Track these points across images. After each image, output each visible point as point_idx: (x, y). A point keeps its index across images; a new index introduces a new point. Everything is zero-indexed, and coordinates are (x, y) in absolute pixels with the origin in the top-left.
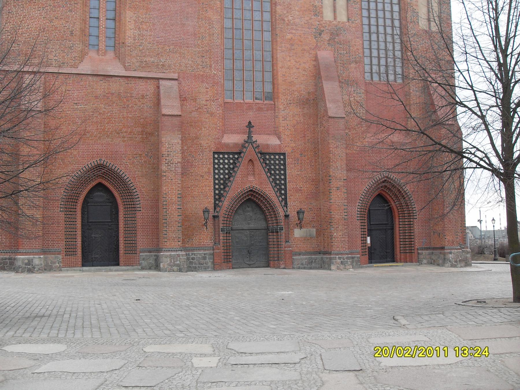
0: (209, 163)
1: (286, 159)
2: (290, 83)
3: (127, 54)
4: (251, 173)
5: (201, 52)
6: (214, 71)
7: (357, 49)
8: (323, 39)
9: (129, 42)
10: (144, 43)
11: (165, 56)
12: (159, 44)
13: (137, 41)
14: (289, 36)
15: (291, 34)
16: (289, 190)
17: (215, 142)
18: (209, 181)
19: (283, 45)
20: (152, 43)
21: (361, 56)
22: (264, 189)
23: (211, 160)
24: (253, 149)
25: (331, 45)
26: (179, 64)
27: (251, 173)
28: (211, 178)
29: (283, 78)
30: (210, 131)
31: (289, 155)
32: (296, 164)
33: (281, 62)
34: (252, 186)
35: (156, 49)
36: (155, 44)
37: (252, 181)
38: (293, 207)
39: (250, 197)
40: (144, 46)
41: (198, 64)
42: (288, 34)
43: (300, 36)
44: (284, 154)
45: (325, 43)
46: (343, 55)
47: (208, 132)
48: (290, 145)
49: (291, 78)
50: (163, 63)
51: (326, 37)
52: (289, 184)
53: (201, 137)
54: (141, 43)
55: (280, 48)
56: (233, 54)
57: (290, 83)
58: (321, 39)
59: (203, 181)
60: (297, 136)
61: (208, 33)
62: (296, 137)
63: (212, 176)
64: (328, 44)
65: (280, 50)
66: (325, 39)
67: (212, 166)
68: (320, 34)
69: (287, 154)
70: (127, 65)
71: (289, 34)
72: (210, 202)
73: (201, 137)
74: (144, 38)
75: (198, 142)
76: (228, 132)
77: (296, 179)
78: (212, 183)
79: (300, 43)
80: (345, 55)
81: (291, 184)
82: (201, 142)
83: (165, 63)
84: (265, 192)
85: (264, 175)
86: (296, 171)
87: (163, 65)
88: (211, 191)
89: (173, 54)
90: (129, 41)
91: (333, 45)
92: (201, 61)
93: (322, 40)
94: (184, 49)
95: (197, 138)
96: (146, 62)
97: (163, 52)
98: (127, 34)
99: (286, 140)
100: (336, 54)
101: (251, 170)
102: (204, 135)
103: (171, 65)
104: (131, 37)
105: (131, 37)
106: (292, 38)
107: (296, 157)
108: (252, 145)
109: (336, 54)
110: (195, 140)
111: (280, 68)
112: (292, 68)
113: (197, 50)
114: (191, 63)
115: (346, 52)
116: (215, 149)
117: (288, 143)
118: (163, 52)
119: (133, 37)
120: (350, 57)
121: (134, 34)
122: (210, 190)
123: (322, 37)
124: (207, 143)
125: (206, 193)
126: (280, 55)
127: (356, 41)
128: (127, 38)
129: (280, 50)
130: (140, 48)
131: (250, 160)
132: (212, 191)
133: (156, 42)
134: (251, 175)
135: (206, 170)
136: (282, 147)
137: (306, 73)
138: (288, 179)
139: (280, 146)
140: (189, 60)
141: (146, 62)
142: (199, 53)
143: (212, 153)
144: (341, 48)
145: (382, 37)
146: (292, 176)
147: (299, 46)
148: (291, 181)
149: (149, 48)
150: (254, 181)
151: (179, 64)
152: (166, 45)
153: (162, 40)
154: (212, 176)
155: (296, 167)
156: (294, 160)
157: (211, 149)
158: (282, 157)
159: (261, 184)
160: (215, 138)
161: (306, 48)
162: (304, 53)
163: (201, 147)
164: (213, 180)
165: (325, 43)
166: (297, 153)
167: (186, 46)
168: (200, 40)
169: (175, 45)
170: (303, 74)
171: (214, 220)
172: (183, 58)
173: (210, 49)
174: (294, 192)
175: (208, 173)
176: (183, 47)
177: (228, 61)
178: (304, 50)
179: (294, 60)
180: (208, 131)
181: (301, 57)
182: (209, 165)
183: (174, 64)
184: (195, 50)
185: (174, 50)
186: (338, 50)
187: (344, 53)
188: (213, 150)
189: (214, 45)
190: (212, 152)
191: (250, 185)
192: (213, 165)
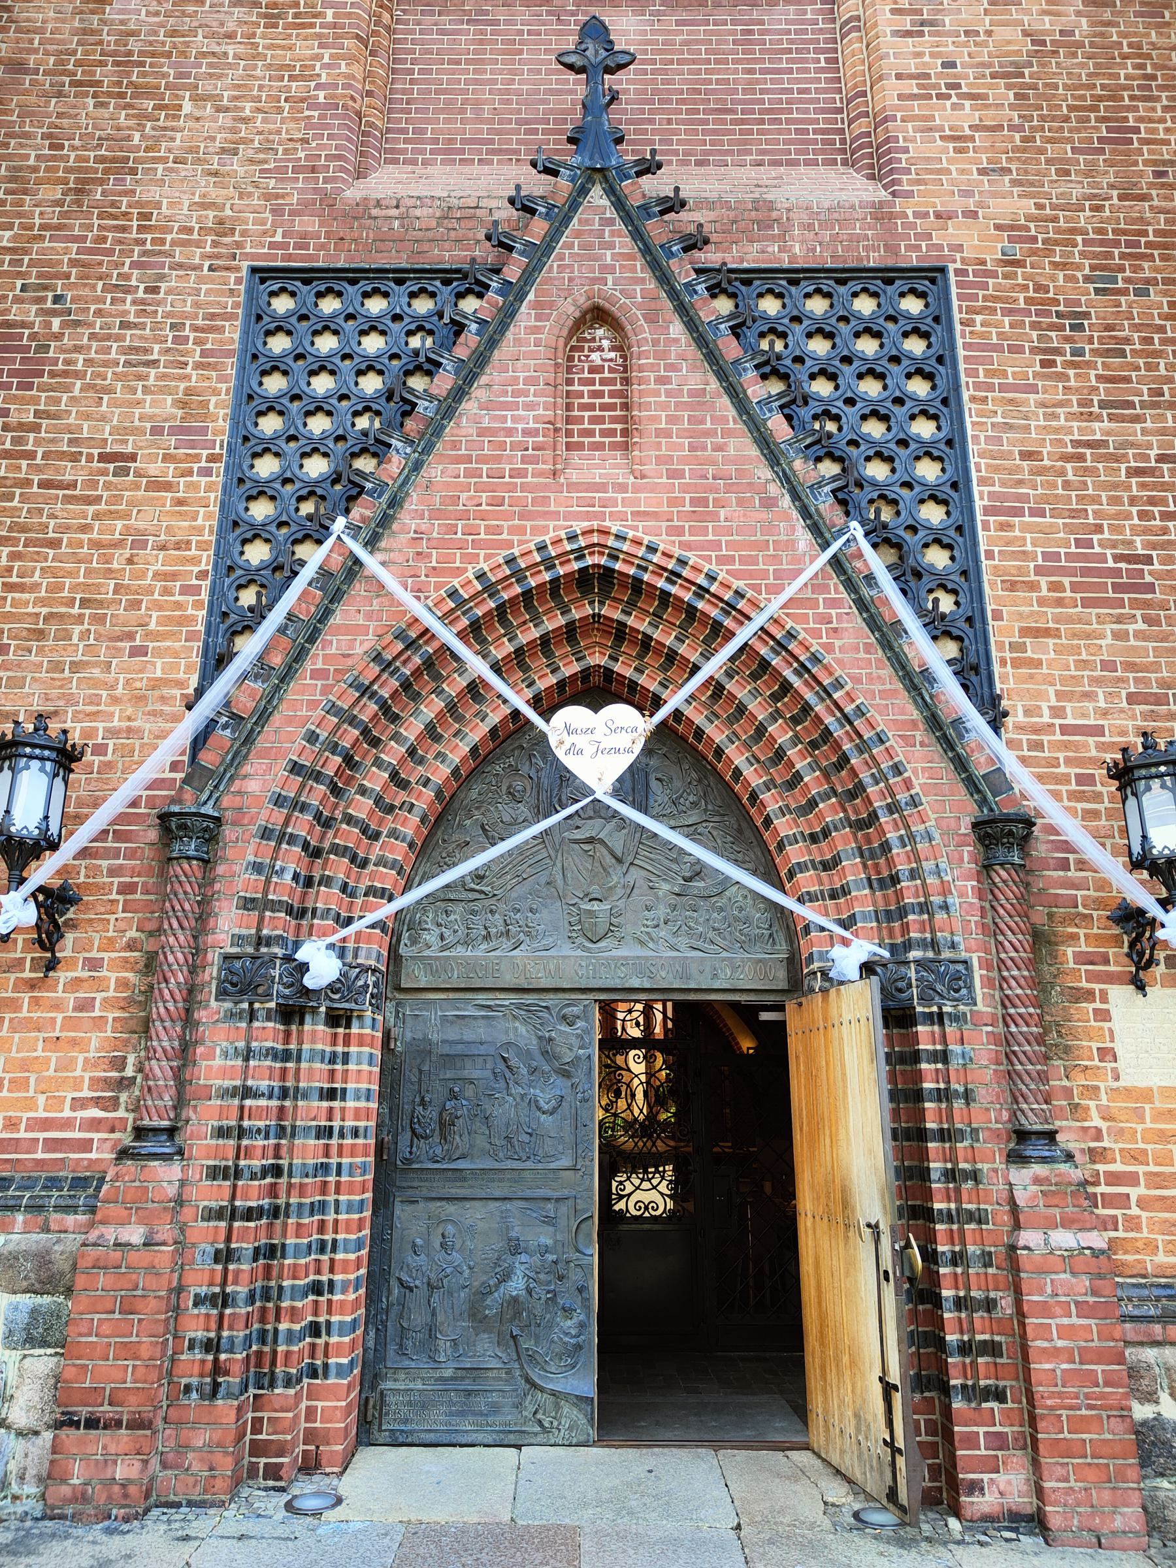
0: (203, 354)
1: (957, 316)
4: (604, 433)
16: (1012, 586)
17: (277, 196)
18: (180, 502)
22: (729, 560)
23: (220, 330)
24: (619, 225)
27: (604, 433)
28: (207, 472)
30: (245, 120)
31: (985, 286)
32: (1058, 351)
34: (604, 532)
37: (602, 488)
38: (1066, 746)
39: (597, 659)
44: (935, 274)
47: (222, 129)
48: (981, 205)
52: (1003, 527)
53: (164, 160)
59: (116, 500)
60: (1050, 140)
62: (1042, 151)
63: (212, 459)
67: (222, 379)
69: (958, 272)
72: (155, 684)
73: (164, 160)
75: (126, 193)
76: (422, 152)
77: (1067, 485)
78: (207, 520)
81: (1025, 528)
82: (154, 193)
84: (739, 594)
85: (727, 433)
86: (1071, 416)
88: (186, 590)
95: (119, 166)
99: (948, 171)
101: (603, 407)
102: (194, 150)
107: (1056, 302)
108: (611, 191)
110: (102, 182)
116: (272, 245)
117: (968, 194)
122: (174, 576)
124: (204, 206)
125: (135, 605)
131: (598, 315)
132: (195, 590)
134: (599, 447)
135: (167, 407)
136: (913, 226)
138: (982, 481)
139: (882, 215)
143: (237, 280)
146: (1026, 455)
148: (1024, 498)
150: (623, 488)
154: (212, 459)
155: (1064, 377)
156: (1034, 326)
157: (239, 245)
158: (912, 306)
159: (701, 512)
160: (277, 169)
163: (141, 229)
164: (214, 497)
166: (1055, 265)
171: (163, 874)
174: (1060, 602)
175: (173, 431)
180: (223, 119)
182: (198, 366)
188: (258, 252)
190: (245, 265)
191: (579, 526)
192: (231, 372)
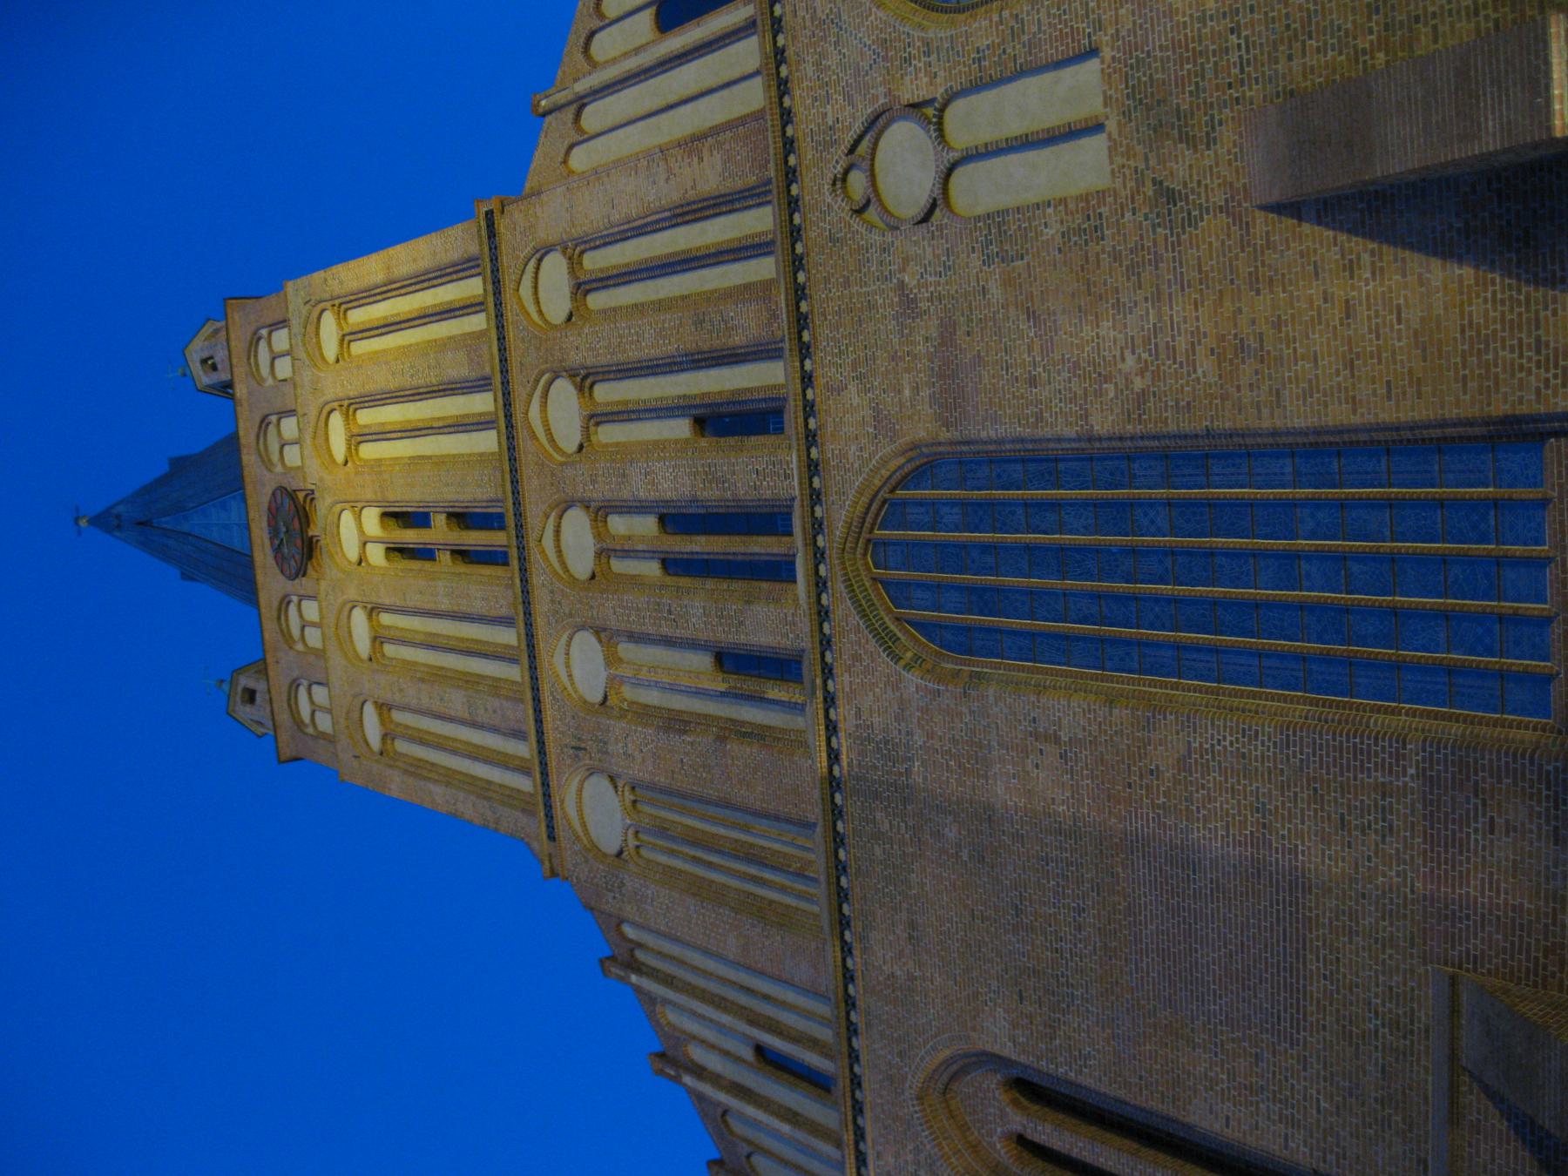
2: (1424, 350)
6: (1405, 774)
14: (1206, 366)
20: (1305, 1050)
25: (1213, 128)
26: (1384, 946)
29: (1404, 393)
42: (1200, 371)
43: (1196, 309)
49: (1397, 344)
50: (1383, 1026)
51: (1181, 166)
55: (1265, 412)
57: (1424, 350)
58: (1193, 192)
66: (1191, 166)
68: (1171, 197)
71: (1195, 371)
93: (1199, 182)
111: (1354, 412)
112: (1349, 343)
123: (1185, 184)
137: (1366, 257)
162: (1271, 280)
170: (1373, 273)
173: (1309, 785)
183: (1384, 973)
189: (1288, 759)
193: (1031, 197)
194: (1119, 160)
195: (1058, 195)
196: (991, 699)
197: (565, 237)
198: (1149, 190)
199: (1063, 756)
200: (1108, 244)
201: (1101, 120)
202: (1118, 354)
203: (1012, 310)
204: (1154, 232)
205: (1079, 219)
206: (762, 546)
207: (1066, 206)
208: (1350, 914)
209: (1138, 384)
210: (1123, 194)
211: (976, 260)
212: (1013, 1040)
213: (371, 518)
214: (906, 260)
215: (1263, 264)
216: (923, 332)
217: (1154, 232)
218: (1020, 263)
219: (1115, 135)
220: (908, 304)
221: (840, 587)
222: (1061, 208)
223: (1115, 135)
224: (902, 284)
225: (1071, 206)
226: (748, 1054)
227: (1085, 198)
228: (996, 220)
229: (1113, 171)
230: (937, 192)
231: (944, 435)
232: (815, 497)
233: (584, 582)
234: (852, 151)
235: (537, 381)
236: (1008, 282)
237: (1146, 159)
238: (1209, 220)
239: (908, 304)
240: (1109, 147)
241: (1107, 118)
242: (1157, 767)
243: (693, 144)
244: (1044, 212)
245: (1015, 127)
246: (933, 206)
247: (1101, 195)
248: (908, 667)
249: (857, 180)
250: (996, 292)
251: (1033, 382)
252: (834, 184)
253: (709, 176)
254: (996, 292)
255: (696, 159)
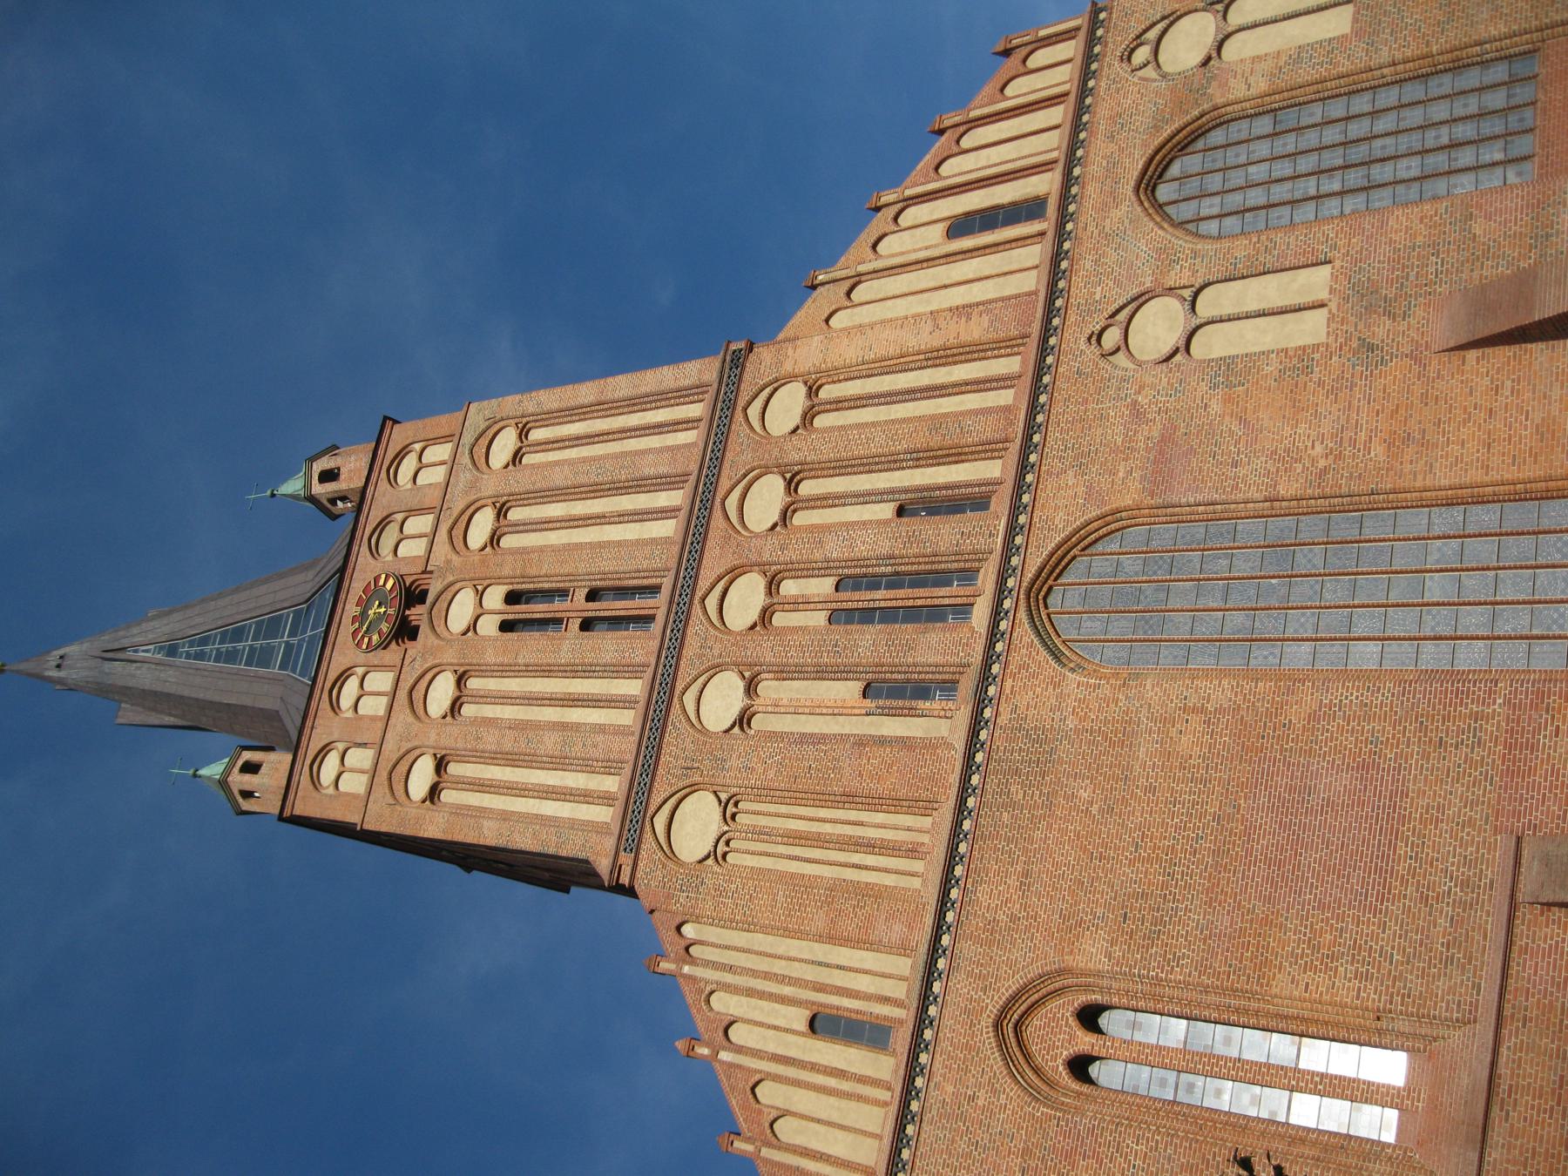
3: (1418, 1009)
5: (1424, 750)
7: (1421, 222)
8: (1388, 336)
9: (1376, 997)
10: (1382, 947)
11: (1431, 875)
12: (1389, 893)
13: (1373, 968)
14: (1378, 451)
15: (1370, 443)
19: (1408, 468)
21: (1444, 204)
25: (1409, 309)
26: (1463, 827)
33: (1466, 470)
35: (1404, 904)
36: (1387, 907)
40: (1393, 948)
41: (1465, 762)
42: (1373, 454)
43: (1377, 415)
45: (1401, 329)
46: (1442, 266)
50: (1456, 886)
51: (1381, 329)
54: (1380, 956)
55: (1420, 477)
56: (1435, 638)
61: (1359, 725)
64: (1404, 320)
65: (1424, 479)
66: (1389, 330)
70: (1455, 1015)
71: (1369, 454)
74: (1366, 942)
79: (1402, 411)
80: (1443, 260)
83: (1457, 877)
87: (1465, 884)
89: (1428, 847)
90: (1372, 996)
91: (1410, 302)
92: (1456, 748)
94: (1411, 807)
96: (1448, 944)
97: (1418, 881)
98: (1349, 1000)
100: (1439, 290)
103: (1465, 857)
104: (1359, 988)
105: (1359, 988)
106: (1385, 441)
109: (1439, 290)
113: (1417, 761)
114: (1463, 785)
115: (1433, 255)
118: (1418, 881)
119: (1360, 982)
120: (1449, 243)
121: (1348, 975)
123: (1383, 341)
126: (1444, 477)
127: (1395, 226)
128: (1362, 1001)
129: (1424, 479)
130: (1397, 960)
133: (1382, 904)
140: (1451, 793)
141: (1448, 944)
142: (1426, 756)
144: (1417, 273)
145: (1383, 147)
147: (1411, 416)
149: (1401, 930)
151: (1463, 827)
152: (1393, 867)
153: (1375, 879)
161: (1418, 389)
165: (1401, 329)
167: (1401, 801)
168: (1381, 749)
169: (1396, 839)
172: (1443, 814)
176: (1405, 809)
177: (1460, 655)
178: (1424, 396)
179: (1459, 430)
181: (1451, 405)
184: (1416, 770)
185: (1413, 842)
186: (1426, 285)
187: (1437, 263)
193: (1256, 349)
194: (1333, 326)
195: (1280, 347)
196: (1149, 687)
197: (812, 369)
198: (1355, 344)
199: (1208, 722)
200: (1315, 377)
201: (1326, 302)
202: (1310, 444)
203: (1227, 418)
204: (1353, 369)
205: (1295, 361)
206: (943, 595)
207: (1286, 353)
208: (1438, 808)
209: (1322, 463)
210: (1334, 345)
211: (1203, 386)
212: (1109, 956)
213: (495, 598)
214: (1142, 388)
215: (1433, 387)
216: (1145, 433)
217: (1353, 369)
218: (1241, 388)
219: (1334, 311)
220: (1137, 413)
221: (1022, 614)
222: (1283, 354)
223: (1334, 311)
224: (1135, 402)
225: (1291, 353)
226: (802, 1026)
227: (1304, 348)
228: (1228, 363)
229: (1328, 333)
230: (1182, 343)
231: (1149, 501)
232: (1009, 549)
233: (740, 633)
234: (1113, 316)
235: (745, 476)
236: (1228, 400)
237: (1356, 326)
238: (1397, 362)
239: (1137, 413)
240: (1329, 319)
241: (1330, 301)
242: (1290, 721)
243: (964, 311)
244: (1268, 357)
245: (1253, 306)
246: (1176, 351)
247: (1316, 347)
248: (1073, 670)
249: (1112, 337)
250: (1215, 407)
251: (1235, 464)
252: (1089, 339)
253: (976, 330)
254: (1215, 407)
255: (964, 319)
